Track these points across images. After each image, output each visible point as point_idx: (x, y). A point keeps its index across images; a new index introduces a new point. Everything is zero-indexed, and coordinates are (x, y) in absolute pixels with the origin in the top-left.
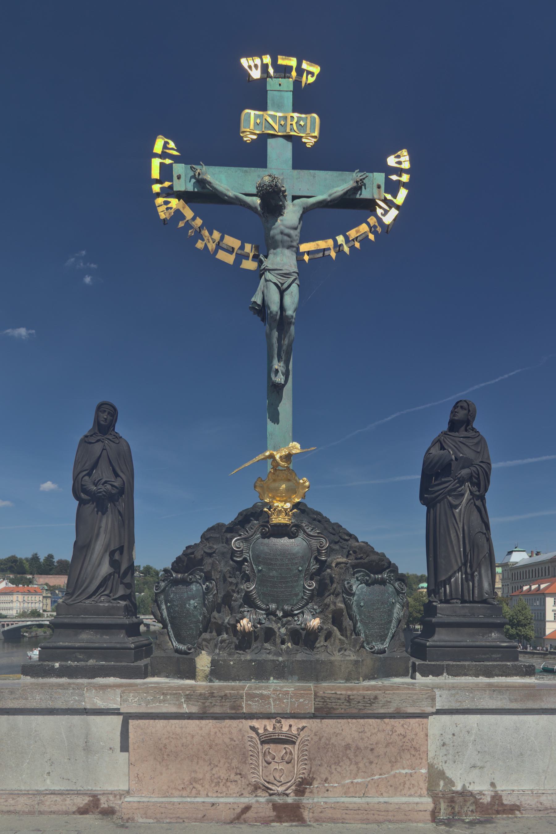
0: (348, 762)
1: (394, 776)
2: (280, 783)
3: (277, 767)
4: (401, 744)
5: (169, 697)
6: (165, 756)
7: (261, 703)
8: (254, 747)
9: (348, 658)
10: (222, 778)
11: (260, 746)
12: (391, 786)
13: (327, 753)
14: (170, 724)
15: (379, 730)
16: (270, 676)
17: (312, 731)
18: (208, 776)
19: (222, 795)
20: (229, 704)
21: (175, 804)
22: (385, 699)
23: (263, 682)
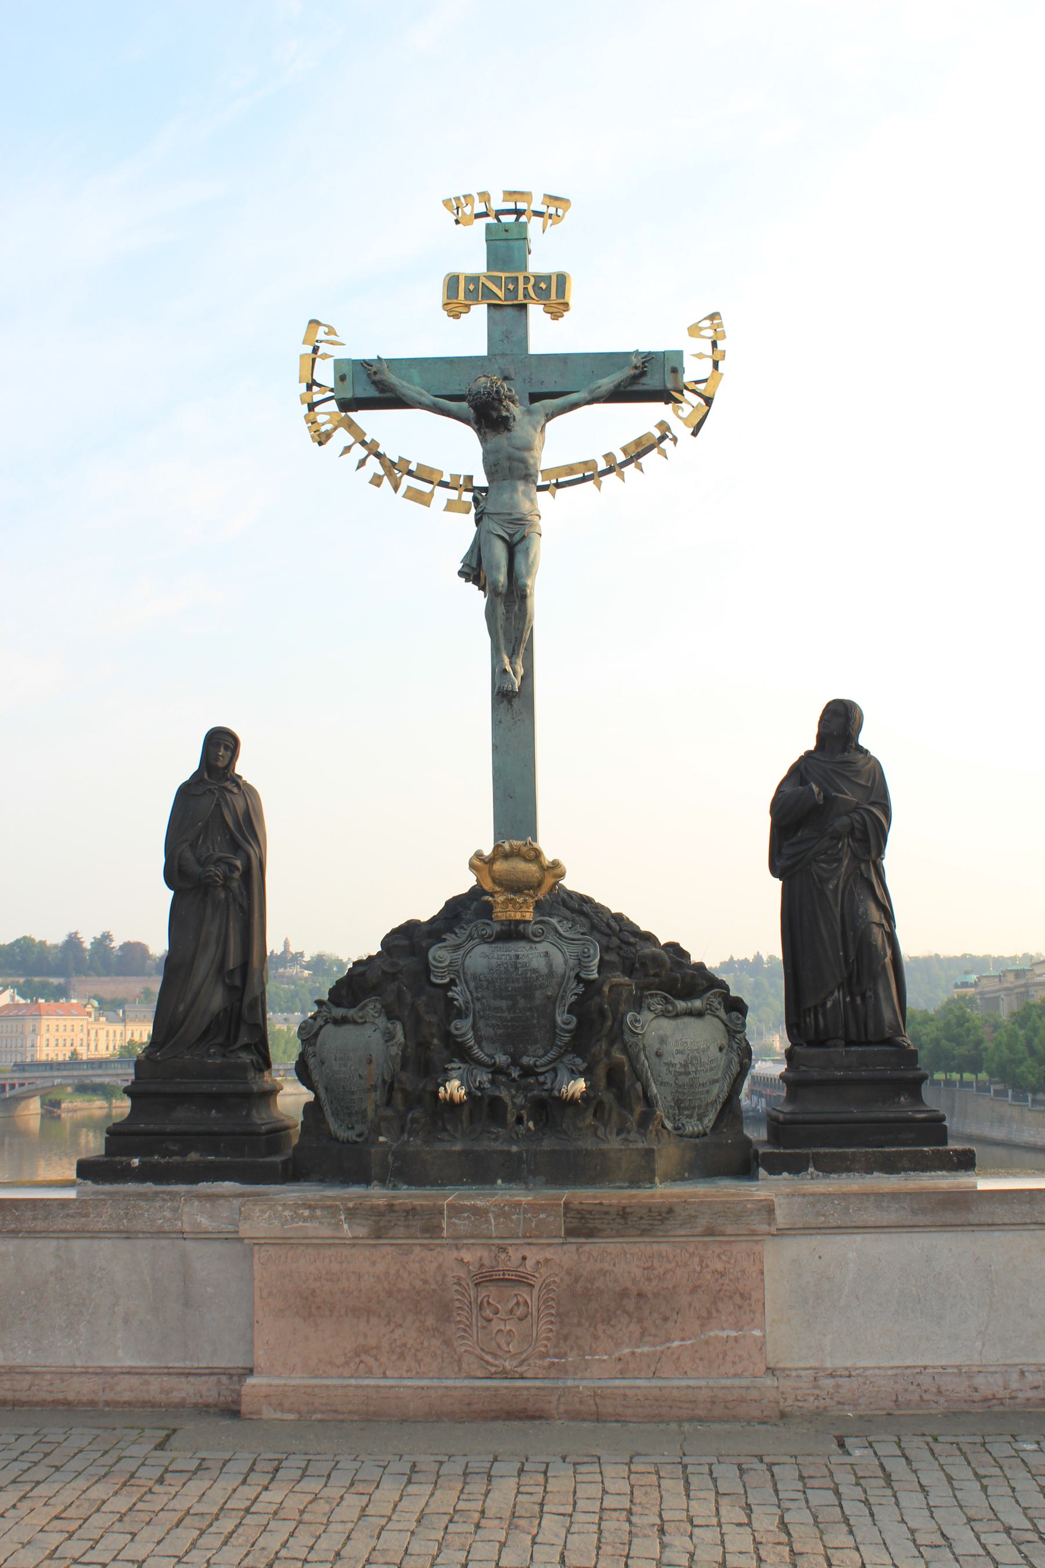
1: (707, 1342)
2: (509, 1355)
4: (718, 1289)
8: (463, 1295)
9: (631, 1146)
10: (409, 1346)
12: (701, 1359)
14: (322, 1256)
15: (677, 1265)
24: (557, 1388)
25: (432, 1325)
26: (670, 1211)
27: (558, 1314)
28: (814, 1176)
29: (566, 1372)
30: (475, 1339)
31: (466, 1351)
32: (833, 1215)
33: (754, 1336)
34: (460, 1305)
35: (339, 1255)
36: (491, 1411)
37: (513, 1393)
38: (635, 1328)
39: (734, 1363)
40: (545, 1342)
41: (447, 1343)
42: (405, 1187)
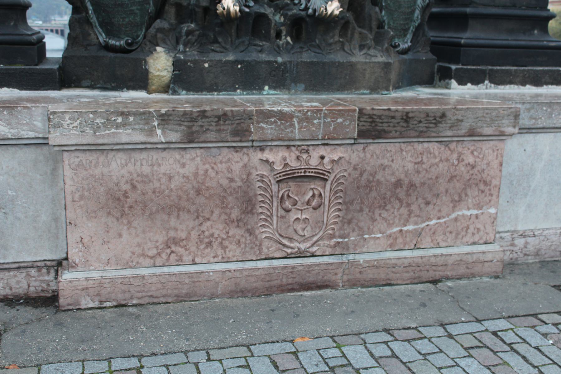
0: (397, 205)
1: (456, 219)
3: (299, 216)
4: (468, 178)
5: (131, 119)
6: (126, 209)
7: (280, 126)
10: (216, 236)
11: (275, 188)
12: (451, 232)
13: (369, 193)
14: (133, 160)
15: (441, 160)
16: (264, 85)
17: (351, 164)
18: (194, 235)
19: (216, 260)
20: (230, 127)
21: (146, 278)
22: (455, 117)
23: (253, 94)
24: (342, 263)
25: (237, 217)
26: (443, 115)
27: (345, 203)
28: (488, 86)
29: (348, 249)
30: (275, 226)
31: (266, 237)
32: (541, 118)
33: (490, 214)
34: (261, 200)
35: (150, 159)
36: (289, 284)
37: (307, 269)
38: (404, 211)
39: (473, 234)
40: (333, 226)
41: (251, 232)
42: (184, 92)
